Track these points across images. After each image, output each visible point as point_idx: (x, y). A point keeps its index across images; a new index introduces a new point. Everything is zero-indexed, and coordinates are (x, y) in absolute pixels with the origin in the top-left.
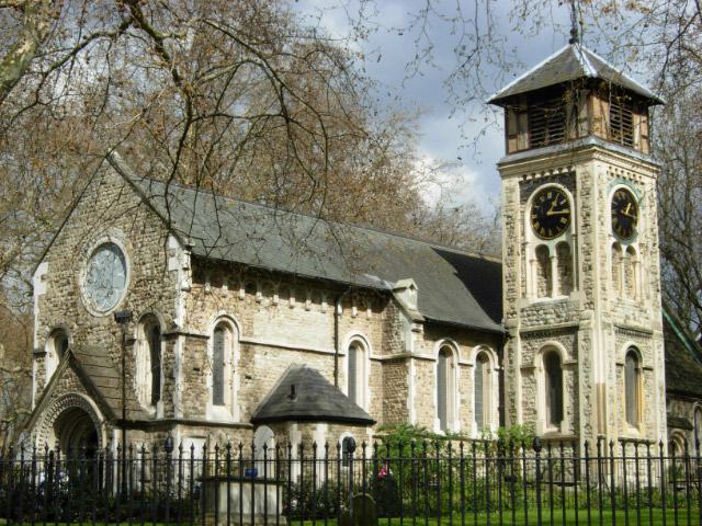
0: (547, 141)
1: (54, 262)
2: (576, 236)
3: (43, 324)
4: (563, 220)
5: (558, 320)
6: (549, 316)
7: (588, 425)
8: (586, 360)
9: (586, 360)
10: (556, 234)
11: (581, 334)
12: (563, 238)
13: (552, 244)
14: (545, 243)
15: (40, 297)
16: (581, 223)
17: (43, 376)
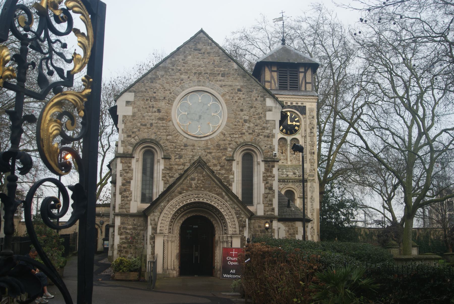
0: (289, 88)
1: (140, 95)
2: (305, 137)
3: (129, 136)
4: (296, 128)
5: (294, 176)
6: (288, 173)
7: (312, 228)
8: (312, 197)
9: (312, 197)
10: (292, 133)
11: (309, 184)
12: (297, 136)
13: (289, 138)
14: (294, 137)
15: (125, 116)
16: (308, 131)
17: (129, 175)
